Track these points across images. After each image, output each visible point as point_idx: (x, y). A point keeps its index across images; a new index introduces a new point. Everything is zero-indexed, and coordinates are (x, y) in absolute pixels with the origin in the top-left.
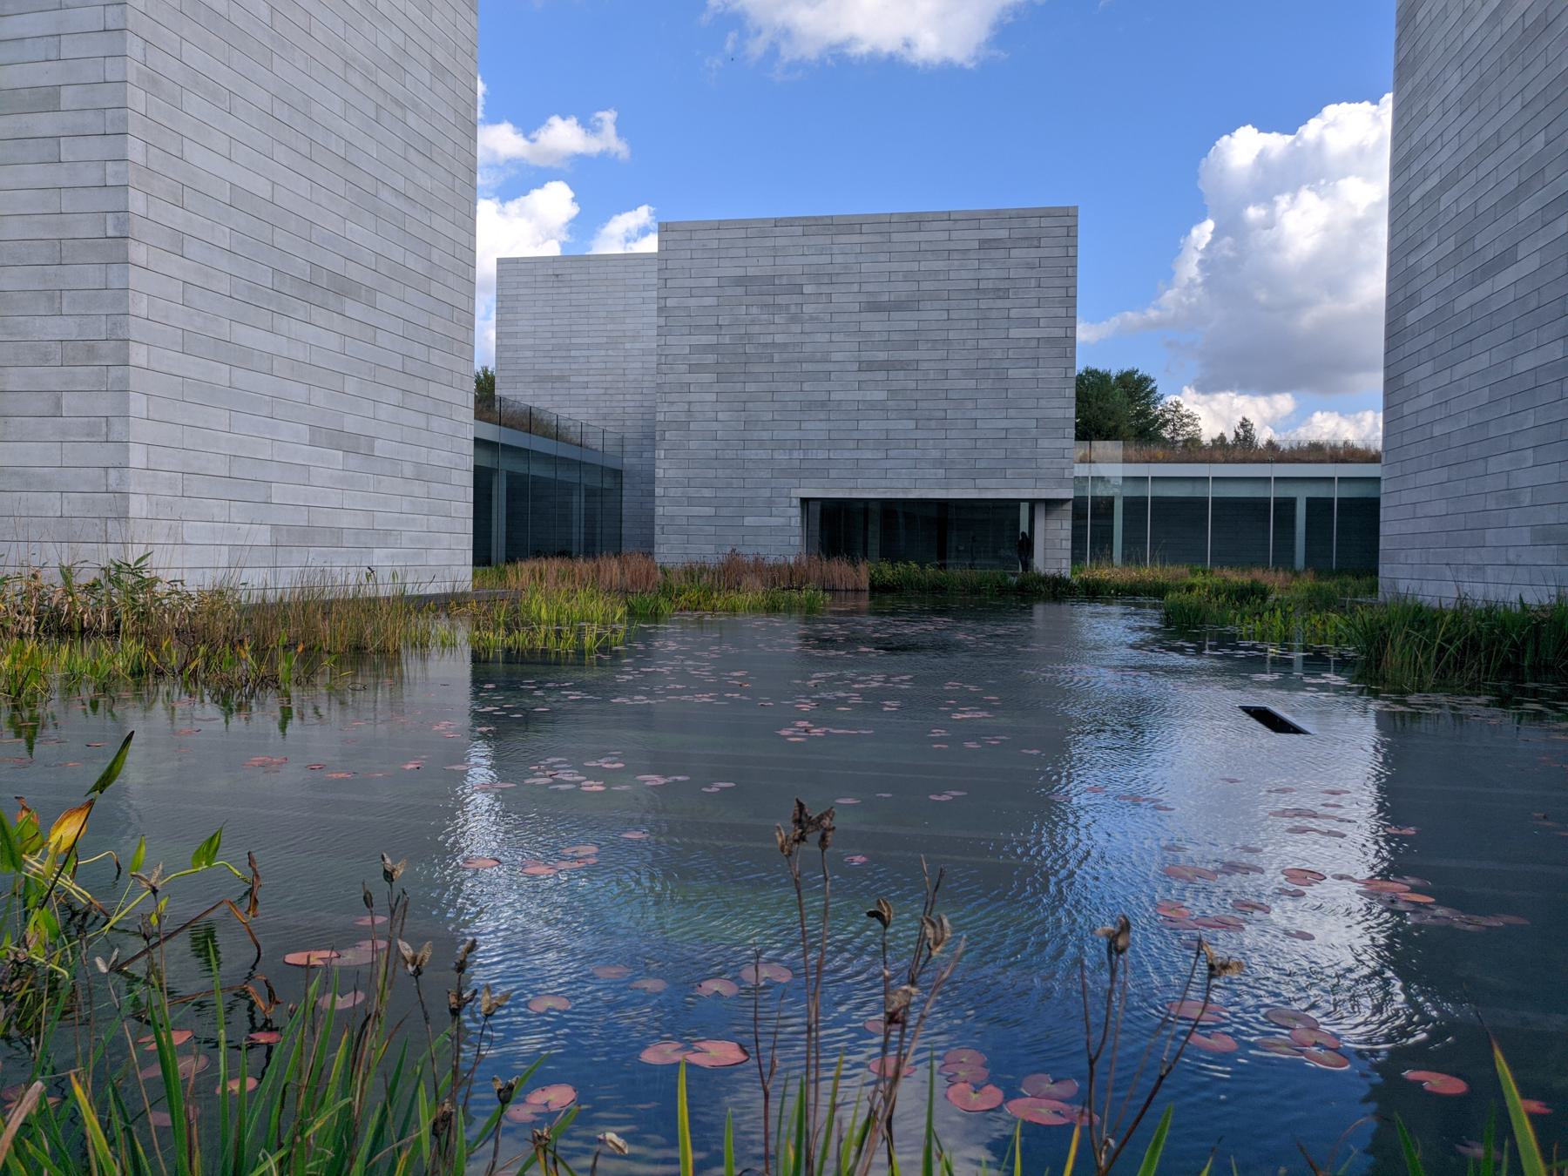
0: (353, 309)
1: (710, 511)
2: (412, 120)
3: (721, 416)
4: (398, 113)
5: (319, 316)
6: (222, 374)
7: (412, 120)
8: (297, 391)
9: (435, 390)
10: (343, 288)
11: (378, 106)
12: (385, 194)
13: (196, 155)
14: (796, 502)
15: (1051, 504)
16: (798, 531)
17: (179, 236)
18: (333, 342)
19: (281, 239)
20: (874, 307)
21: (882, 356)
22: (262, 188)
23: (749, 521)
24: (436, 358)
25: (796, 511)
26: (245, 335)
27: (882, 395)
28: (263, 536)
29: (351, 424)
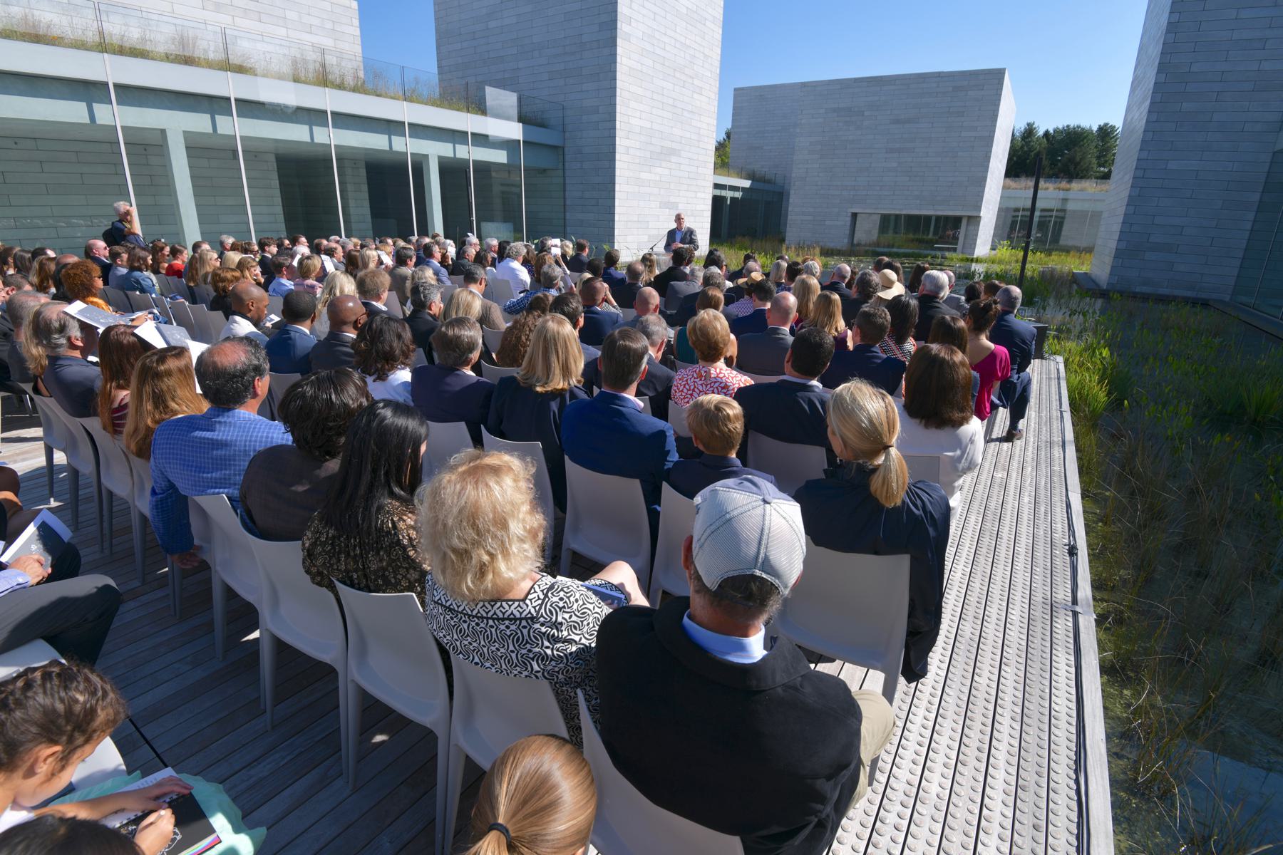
0: (674, 159)
1: (810, 218)
2: (696, 82)
3: (820, 175)
4: (690, 81)
5: (664, 164)
7: (696, 82)
10: (672, 152)
11: (684, 82)
12: (685, 114)
14: (850, 214)
16: (848, 228)
18: (667, 172)
22: (648, 125)
23: (827, 223)
24: (700, 170)
26: (644, 176)
27: (895, 165)
29: (672, 199)
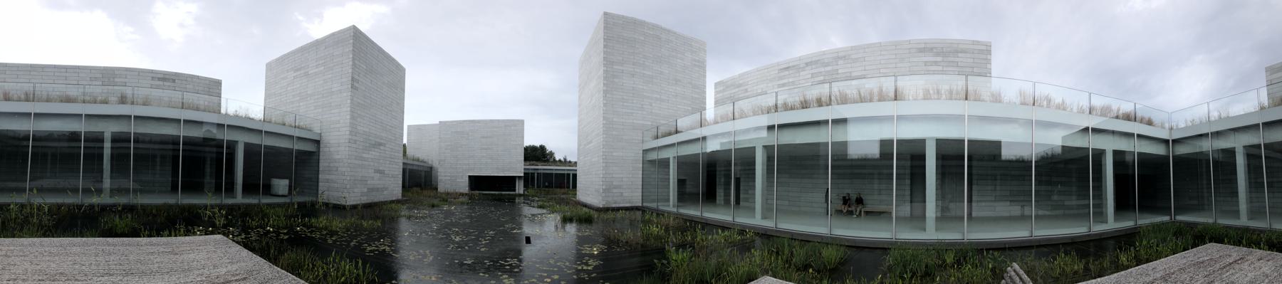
0: (382, 148)
5: (376, 150)
6: (360, 162)
8: (372, 164)
9: (396, 160)
10: (380, 144)
13: (359, 128)
15: (520, 177)
17: (356, 141)
18: (378, 154)
19: (370, 138)
20: (484, 137)
21: (486, 147)
22: (367, 130)
25: (467, 179)
26: (364, 155)
28: (366, 190)
29: (381, 168)
